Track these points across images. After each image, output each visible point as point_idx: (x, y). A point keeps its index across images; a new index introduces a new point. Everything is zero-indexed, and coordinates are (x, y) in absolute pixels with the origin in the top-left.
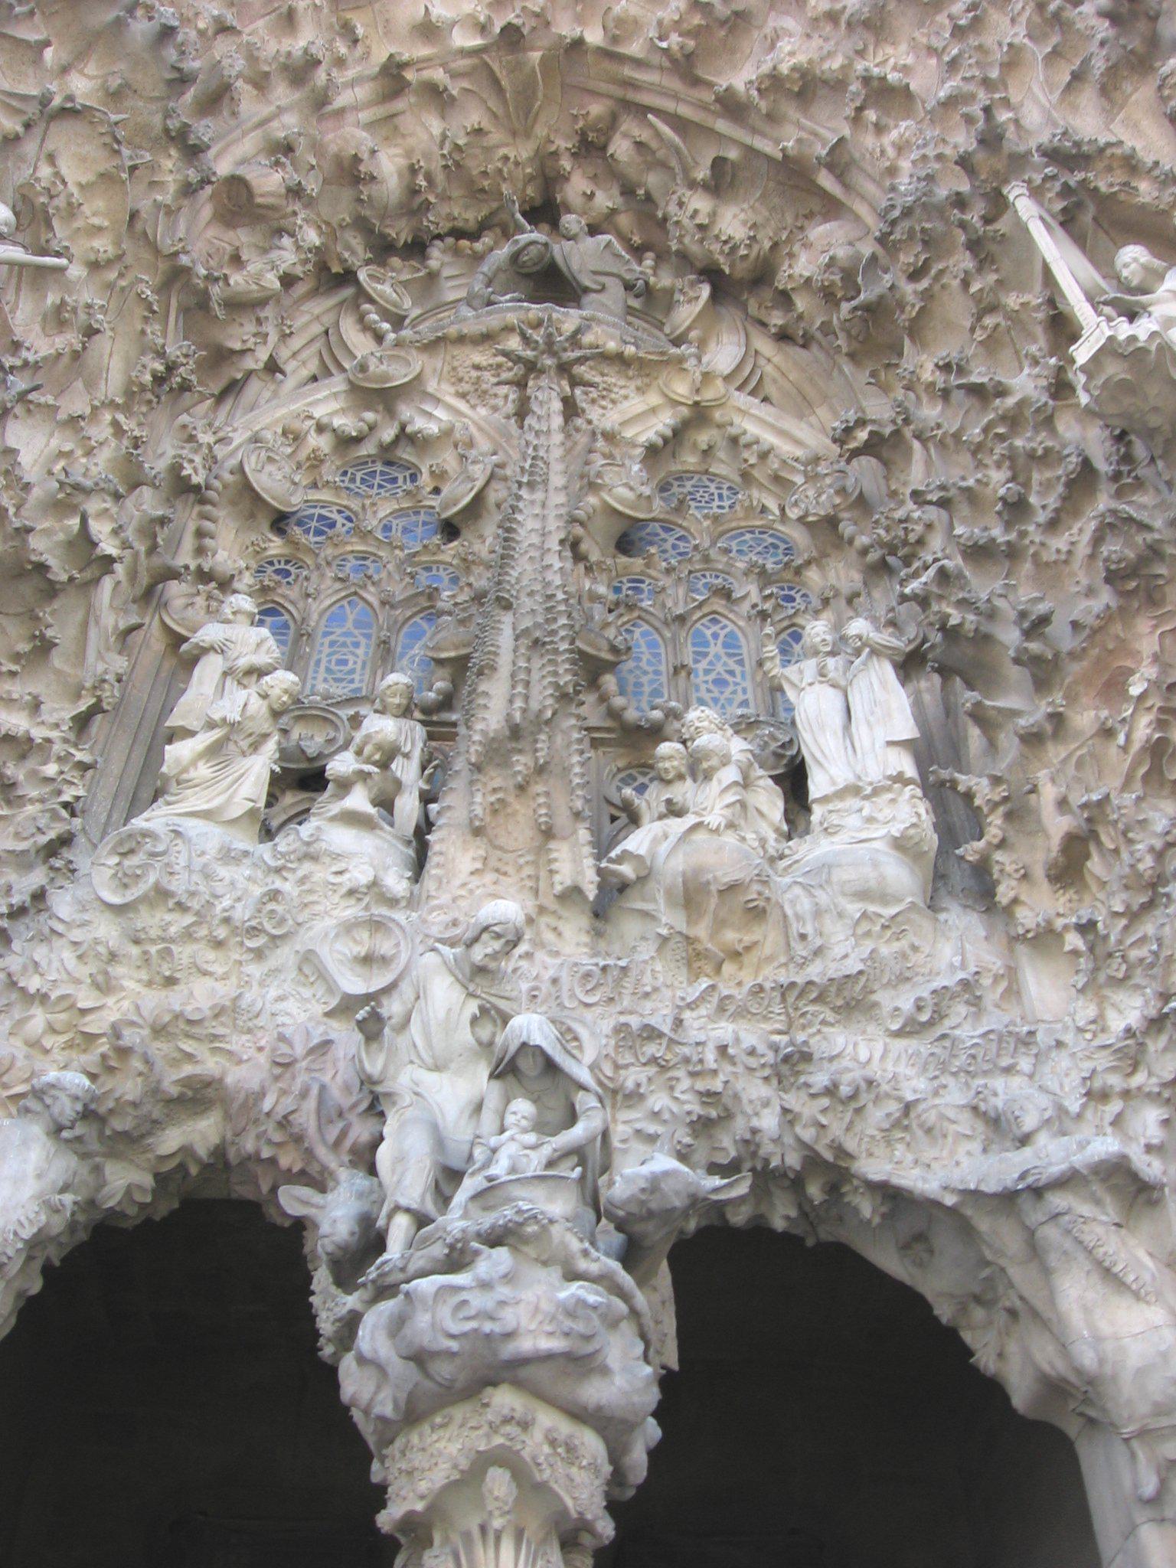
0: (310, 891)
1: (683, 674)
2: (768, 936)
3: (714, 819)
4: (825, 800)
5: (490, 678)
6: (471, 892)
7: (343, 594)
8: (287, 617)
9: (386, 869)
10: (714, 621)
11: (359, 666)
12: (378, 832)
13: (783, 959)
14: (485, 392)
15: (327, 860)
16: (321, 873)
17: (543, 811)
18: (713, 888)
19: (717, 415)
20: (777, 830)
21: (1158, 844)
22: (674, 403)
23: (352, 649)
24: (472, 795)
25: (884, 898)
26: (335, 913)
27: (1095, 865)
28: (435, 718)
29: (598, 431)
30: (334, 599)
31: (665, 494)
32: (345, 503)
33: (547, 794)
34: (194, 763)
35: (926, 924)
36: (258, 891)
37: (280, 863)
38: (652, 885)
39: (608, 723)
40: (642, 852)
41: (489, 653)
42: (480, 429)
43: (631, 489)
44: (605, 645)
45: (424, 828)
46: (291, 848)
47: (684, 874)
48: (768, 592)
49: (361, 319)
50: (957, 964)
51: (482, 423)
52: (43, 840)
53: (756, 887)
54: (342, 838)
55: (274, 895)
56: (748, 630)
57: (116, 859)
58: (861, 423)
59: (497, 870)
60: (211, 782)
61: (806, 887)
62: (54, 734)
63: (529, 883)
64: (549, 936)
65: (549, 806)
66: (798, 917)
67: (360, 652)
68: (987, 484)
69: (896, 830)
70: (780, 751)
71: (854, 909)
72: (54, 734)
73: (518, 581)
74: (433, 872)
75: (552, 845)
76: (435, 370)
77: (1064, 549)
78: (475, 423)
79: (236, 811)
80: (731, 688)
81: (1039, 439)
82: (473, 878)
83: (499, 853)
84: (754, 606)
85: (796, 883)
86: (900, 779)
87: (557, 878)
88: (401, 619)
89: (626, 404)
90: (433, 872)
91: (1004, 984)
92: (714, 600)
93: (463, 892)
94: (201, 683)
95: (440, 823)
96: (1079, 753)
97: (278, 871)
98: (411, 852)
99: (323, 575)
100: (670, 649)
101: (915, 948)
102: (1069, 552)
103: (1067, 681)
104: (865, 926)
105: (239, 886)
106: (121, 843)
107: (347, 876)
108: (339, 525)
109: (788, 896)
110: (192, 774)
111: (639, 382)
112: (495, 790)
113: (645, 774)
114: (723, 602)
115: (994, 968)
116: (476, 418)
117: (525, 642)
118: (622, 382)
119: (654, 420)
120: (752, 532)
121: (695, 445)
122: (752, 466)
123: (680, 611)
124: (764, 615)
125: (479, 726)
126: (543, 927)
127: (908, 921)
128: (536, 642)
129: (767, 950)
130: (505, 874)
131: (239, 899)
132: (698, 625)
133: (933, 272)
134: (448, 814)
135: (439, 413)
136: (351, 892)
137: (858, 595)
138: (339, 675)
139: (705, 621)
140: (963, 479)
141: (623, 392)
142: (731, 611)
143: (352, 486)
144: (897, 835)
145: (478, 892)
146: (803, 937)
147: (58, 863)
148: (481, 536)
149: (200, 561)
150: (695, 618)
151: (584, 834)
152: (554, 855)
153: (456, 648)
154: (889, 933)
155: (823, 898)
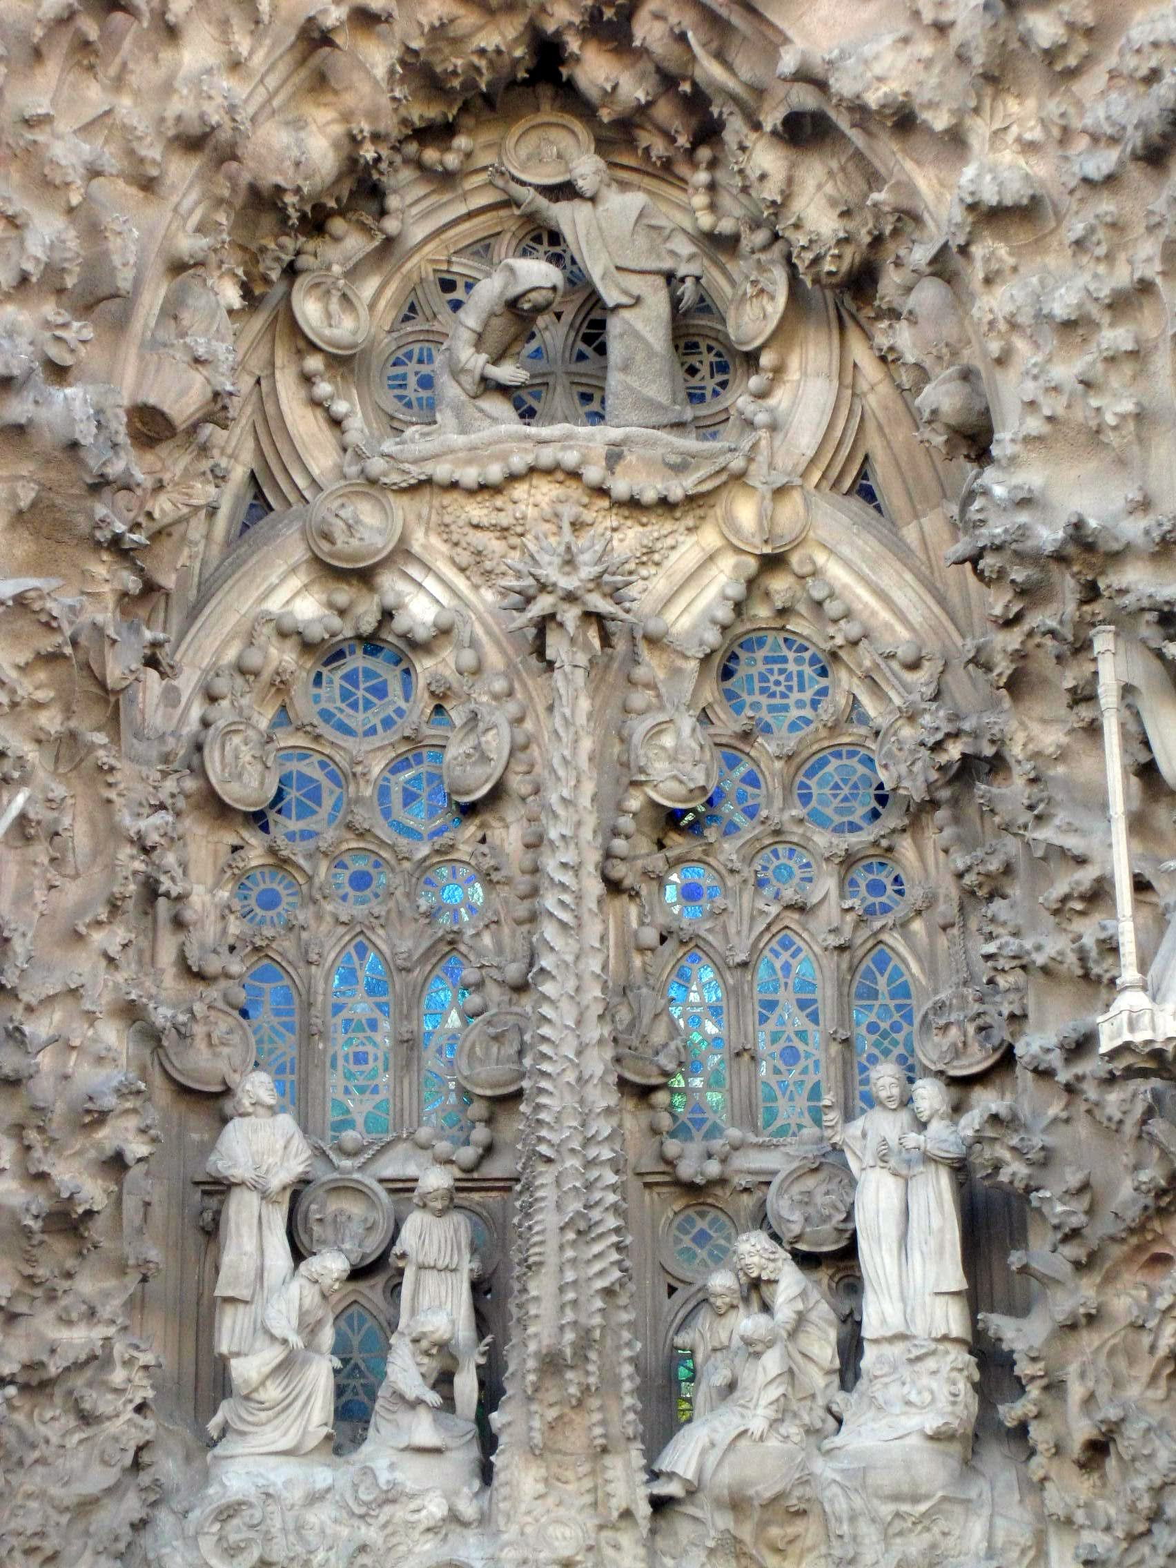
0: (393, 1534)
1: (746, 1057)
2: (809, 1530)
3: (757, 1424)
4: (876, 1341)
5: (537, 1273)
6: (537, 1520)
7: (347, 938)
8: (287, 982)
9: (457, 1493)
10: (786, 944)
11: (380, 1064)
12: (448, 1454)
13: (823, 1549)
14: (490, 572)
15: (404, 1499)
16: (400, 1513)
17: (598, 1431)
18: (756, 1503)
19: (795, 559)
20: (829, 1373)
21: (1158, 1482)
22: (738, 551)
23: (369, 1033)
24: (530, 1414)
25: (915, 1499)
26: (417, 1550)
27: (1111, 1464)
28: (476, 1175)
29: (639, 635)
30: (337, 949)
31: (728, 684)
32: (327, 751)
33: (601, 1408)
34: (263, 1383)
35: (958, 1509)
36: (345, 1532)
37: (363, 1510)
38: (700, 1495)
39: (662, 1168)
40: (690, 1475)
41: (535, 1245)
42: (489, 632)
43: (681, 782)
44: (655, 1070)
45: (488, 1441)
46: (371, 1497)
47: (729, 1487)
48: (847, 904)
49: (307, 379)
50: (982, 1554)
51: (490, 620)
52: (128, 1460)
53: (797, 1493)
54: (412, 1474)
55: (363, 1548)
56: (824, 962)
57: (217, 1526)
58: (955, 735)
59: (558, 1480)
60: (283, 1407)
61: (843, 1487)
62: (111, 1331)
63: (588, 1499)
64: (609, 1552)
65: (603, 1423)
66: (839, 1520)
67: (378, 1037)
68: (1061, 963)
69: (932, 1423)
70: (841, 1226)
71: (886, 1510)
72: (111, 1331)
73: (558, 1119)
74: (501, 1505)
75: (608, 1460)
76: (419, 516)
77: (1117, 1116)
78: (480, 619)
79: (312, 1442)
80: (802, 1063)
81: (1105, 966)
82: (539, 1502)
83: (558, 1457)
84: (835, 931)
85: (834, 1481)
86: (945, 1338)
87: (614, 1502)
88: (420, 980)
89: (674, 556)
90: (501, 1505)
91: (1031, 1554)
92: (788, 913)
93: (529, 1519)
94: (240, 1236)
95: (503, 1440)
96: (1112, 1342)
97: (362, 1517)
98: (475, 1452)
99: (319, 917)
100: (732, 1002)
101: (945, 1534)
102: (1121, 1122)
103: (1107, 1265)
104: (898, 1525)
105: (329, 1531)
106: (221, 1512)
107: (424, 1513)
108: (325, 795)
109: (828, 1493)
110: (261, 1395)
111: (690, 522)
112: (551, 1405)
113: (702, 1215)
114: (796, 916)
115: (1022, 1541)
116: (481, 608)
117: (571, 1236)
118: (668, 526)
119: (713, 571)
120: (838, 755)
121: (767, 594)
122: (841, 647)
123: (742, 957)
124: (841, 949)
125: (532, 1347)
126: (603, 1544)
127: (939, 1511)
128: (579, 1233)
129: (809, 1542)
130: (566, 1482)
131: (331, 1548)
132: (766, 952)
133: (1026, 627)
134: (510, 1430)
135: (430, 583)
136: (428, 1530)
137: (953, 925)
138: (362, 1082)
139: (774, 944)
140: (1039, 948)
141: (670, 541)
142: (806, 929)
143: (330, 707)
144: (930, 1433)
145: (543, 1520)
146: (841, 1537)
147: (145, 1478)
148: (502, 819)
149: (181, 937)
150: (761, 945)
151: (637, 1459)
152: (610, 1475)
153: (492, 1086)
154: (919, 1527)
155: (858, 1502)
